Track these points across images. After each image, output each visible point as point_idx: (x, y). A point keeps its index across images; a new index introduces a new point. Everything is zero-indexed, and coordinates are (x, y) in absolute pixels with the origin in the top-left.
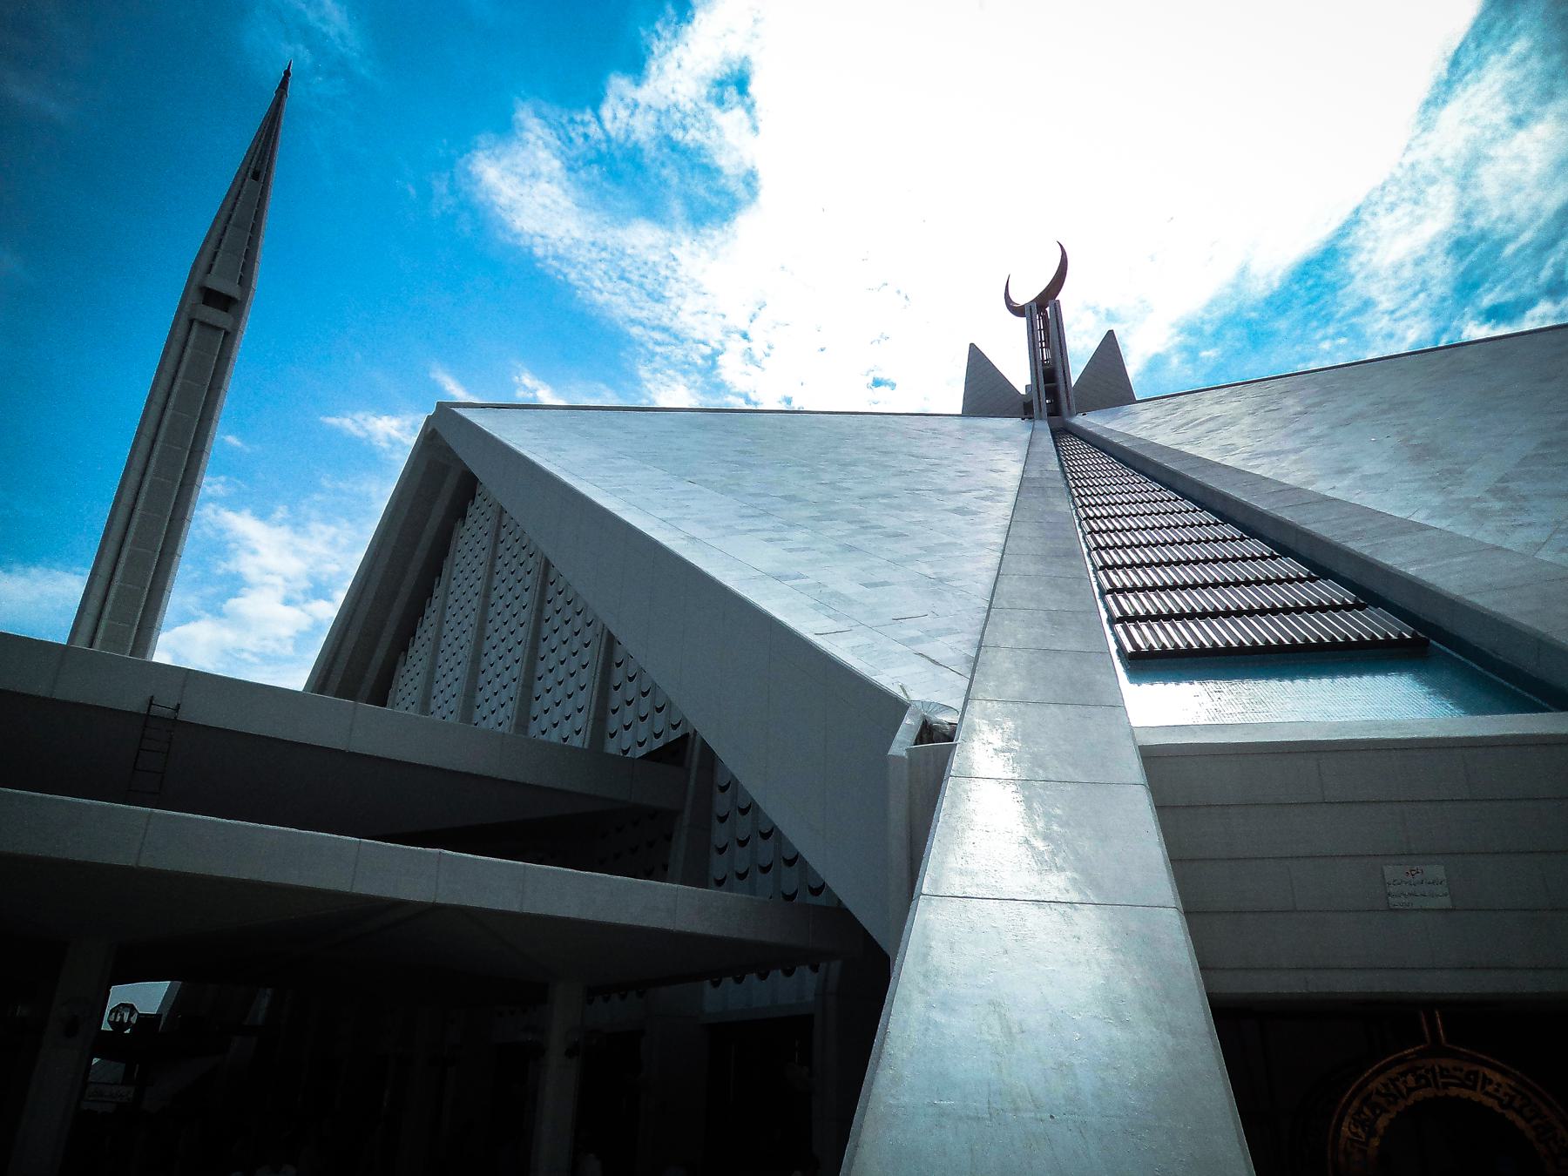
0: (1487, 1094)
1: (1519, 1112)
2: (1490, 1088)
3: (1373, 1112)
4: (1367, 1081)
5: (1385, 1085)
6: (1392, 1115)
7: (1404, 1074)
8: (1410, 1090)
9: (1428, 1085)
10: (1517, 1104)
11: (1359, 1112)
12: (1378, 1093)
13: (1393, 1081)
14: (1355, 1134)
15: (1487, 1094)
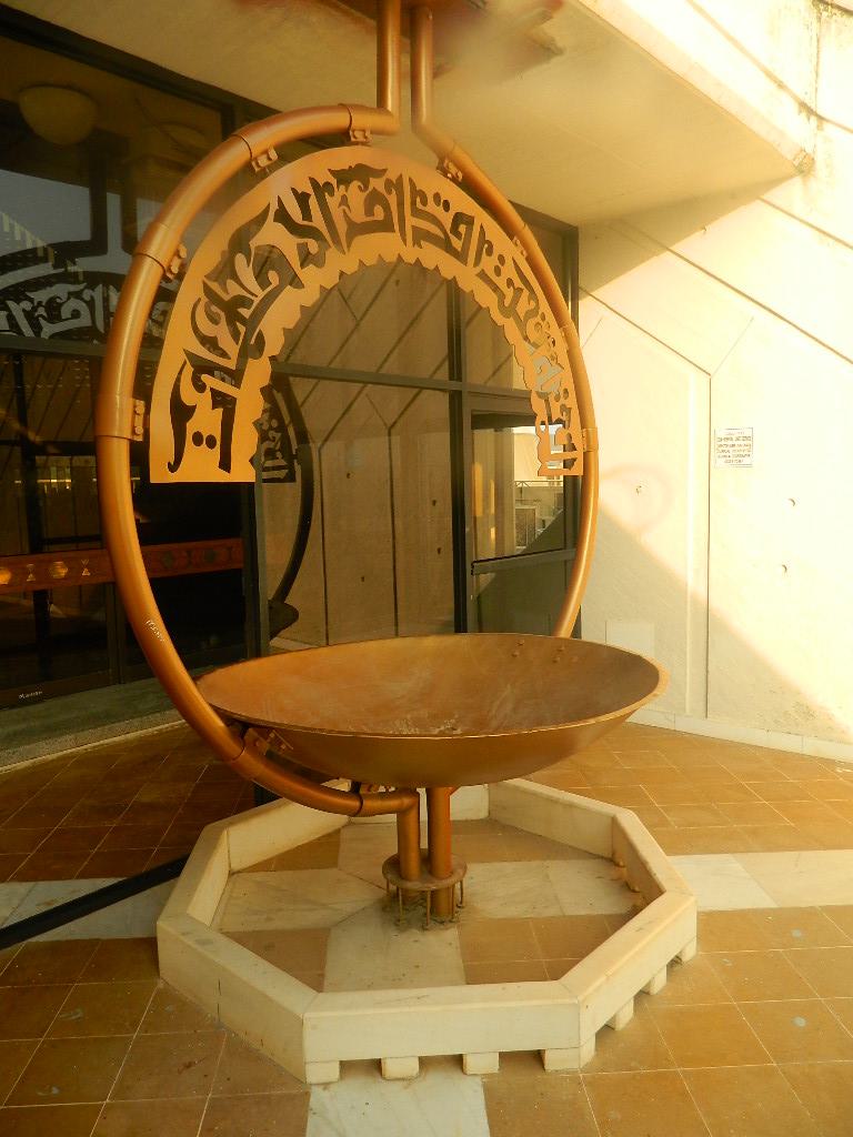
0: (483, 275)
1: (521, 324)
2: (488, 263)
3: (262, 279)
4: (249, 175)
5: (302, 199)
6: (309, 295)
7: (344, 177)
8: (356, 229)
9: (385, 226)
10: (524, 306)
11: (226, 271)
12: (282, 216)
13: (321, 190)
14: (210, 342)
15: (483, 275)
